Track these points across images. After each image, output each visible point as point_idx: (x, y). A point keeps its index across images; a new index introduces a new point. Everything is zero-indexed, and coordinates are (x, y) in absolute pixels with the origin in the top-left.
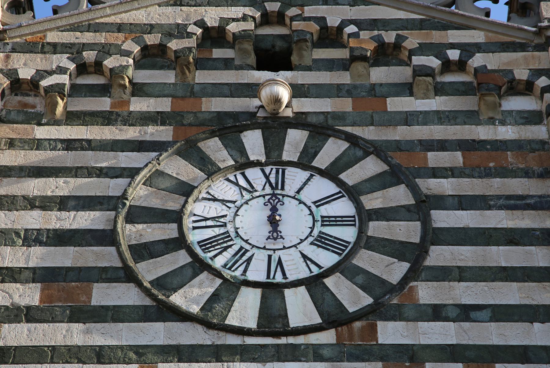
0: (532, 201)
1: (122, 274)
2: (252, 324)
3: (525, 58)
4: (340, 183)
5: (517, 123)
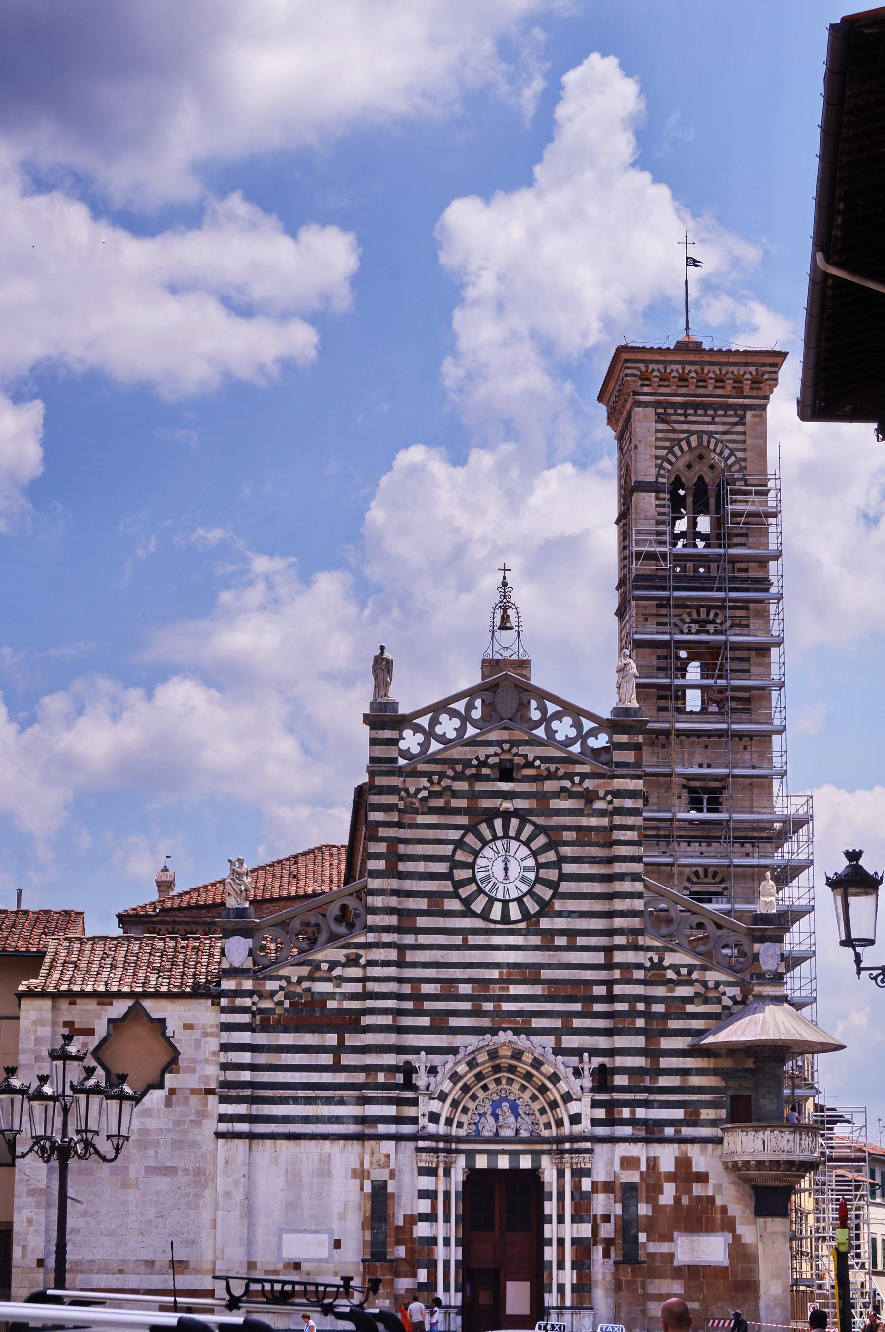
0: (597, 859)
1: (454, 895)
2: (499, 919)
3: (604, 782)
4: (530, 849)
5: (597, 816)
